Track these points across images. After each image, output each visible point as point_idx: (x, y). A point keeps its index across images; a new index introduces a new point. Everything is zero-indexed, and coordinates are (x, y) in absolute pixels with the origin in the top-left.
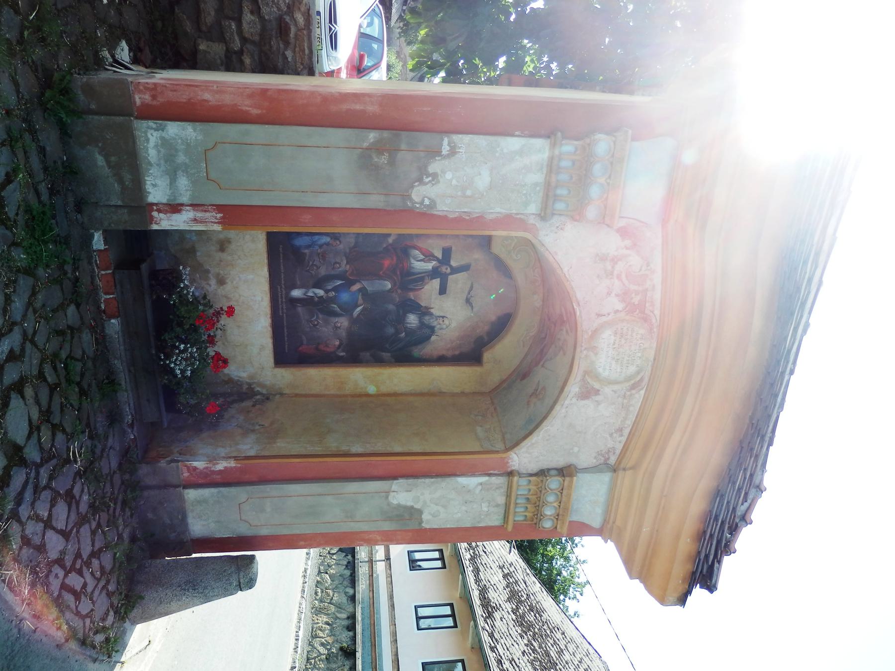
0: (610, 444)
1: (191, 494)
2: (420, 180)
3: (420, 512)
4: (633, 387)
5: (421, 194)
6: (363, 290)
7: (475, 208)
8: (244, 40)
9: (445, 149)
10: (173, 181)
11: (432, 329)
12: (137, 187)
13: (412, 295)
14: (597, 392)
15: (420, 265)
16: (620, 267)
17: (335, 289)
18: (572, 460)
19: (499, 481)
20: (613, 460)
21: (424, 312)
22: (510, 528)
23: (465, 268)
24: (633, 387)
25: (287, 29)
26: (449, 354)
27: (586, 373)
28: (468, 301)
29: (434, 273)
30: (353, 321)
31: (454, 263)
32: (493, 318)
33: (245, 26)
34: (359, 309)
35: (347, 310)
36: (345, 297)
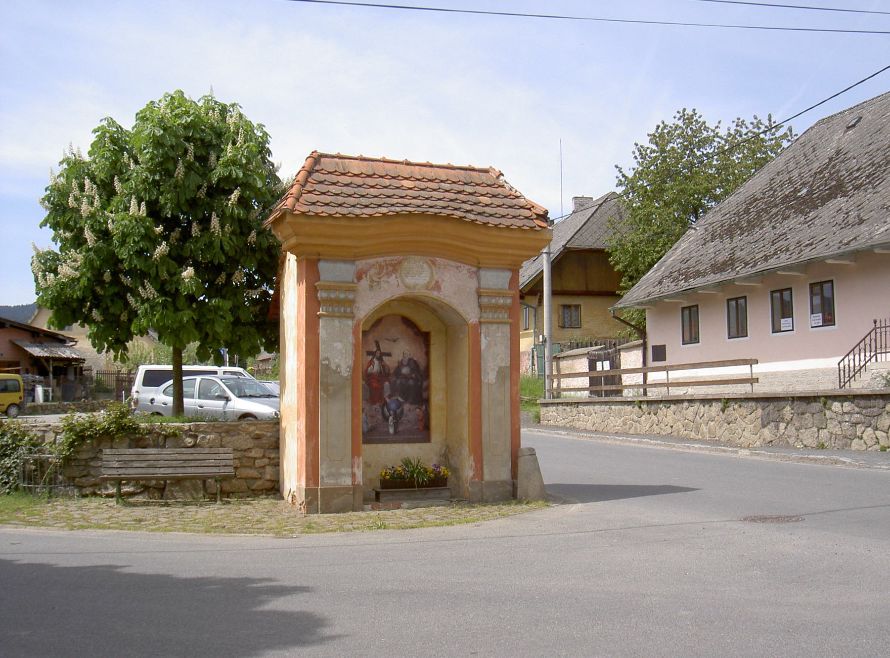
0: (465, 272)
1: (487, 477)
2: (339, 373)
3: (500, 368)
4: (434, 264)
5: (345, 372)
6: (390, 396)
7: (350, 348)
8: (264, 456)
9: (326, 362)
10: (344, 475)
11: (410, 359)
12: (346, 489)
13: (392, 371)
14: (437, 282)
15: (376, 367)
16: (375, 279)
17: (389, 411)
18: (474, 290)
19: (484, 328)
20: (474, 269)
21: (401, 365)
22: (510, 321)
23: (377, 343)
24: (434, 264)
25: (257, 435)
26: (424, 350)
27: (427, 289)
28: (394, 341)
29: (380, 359)
30: (406, 400)
31: (375, 350)
32: (404, 327)
33: (257, 456)
34: (400, 399)
35: (400, 405)
36: (393, 406)
